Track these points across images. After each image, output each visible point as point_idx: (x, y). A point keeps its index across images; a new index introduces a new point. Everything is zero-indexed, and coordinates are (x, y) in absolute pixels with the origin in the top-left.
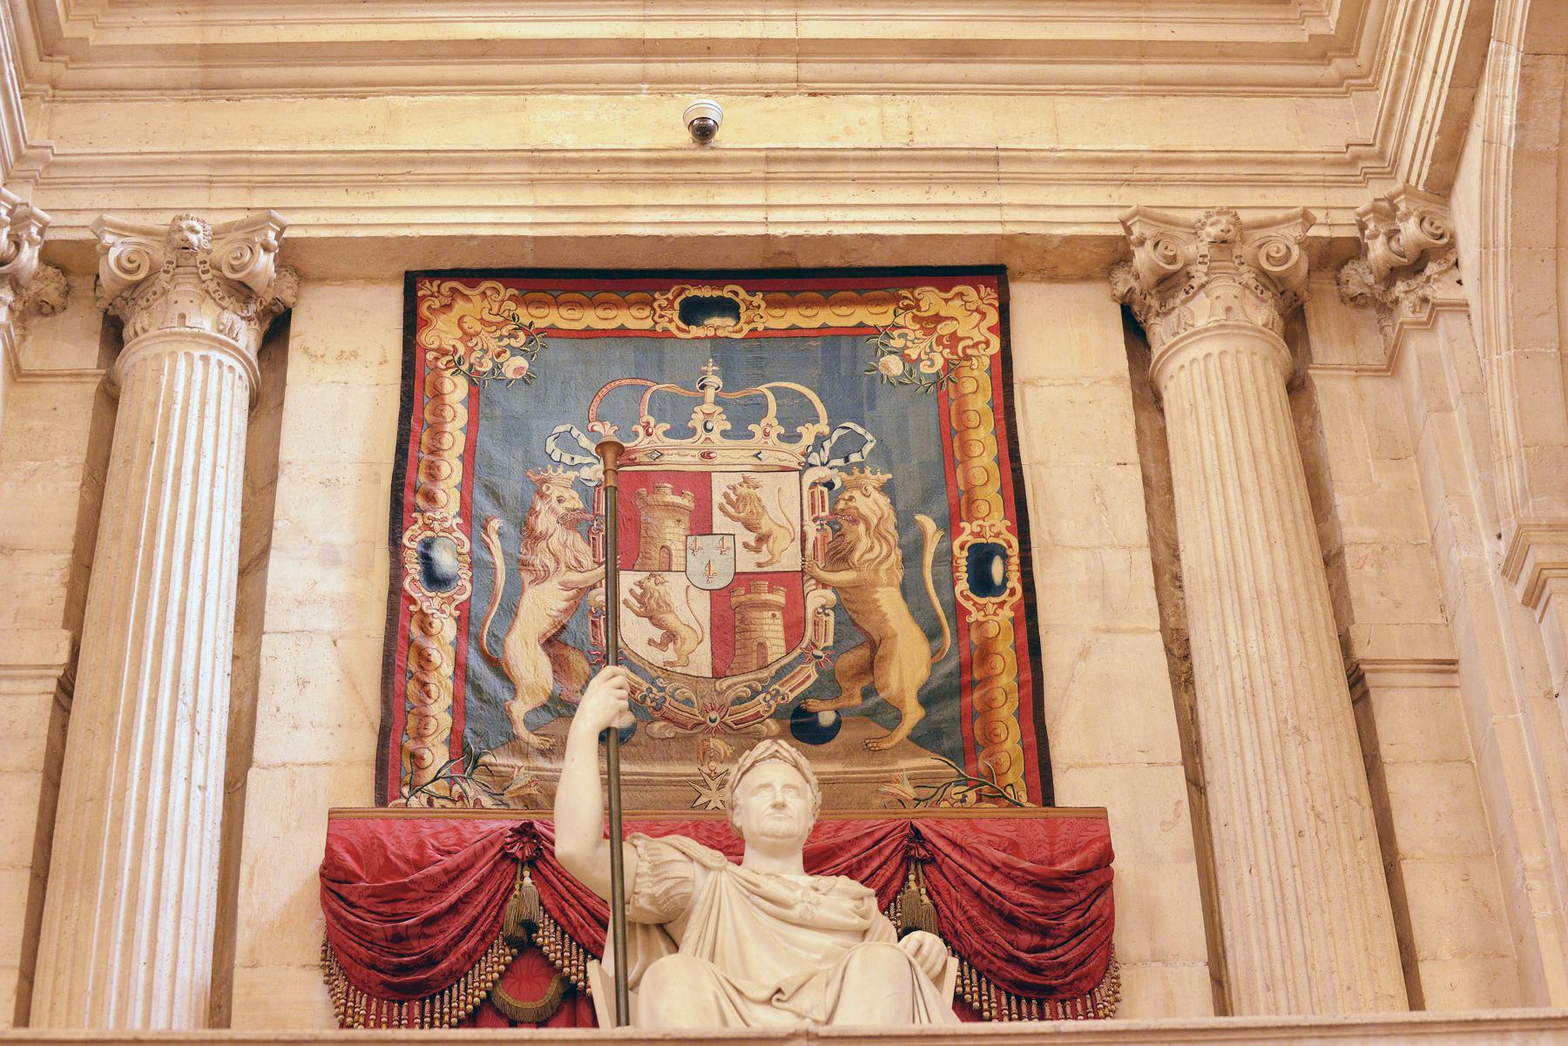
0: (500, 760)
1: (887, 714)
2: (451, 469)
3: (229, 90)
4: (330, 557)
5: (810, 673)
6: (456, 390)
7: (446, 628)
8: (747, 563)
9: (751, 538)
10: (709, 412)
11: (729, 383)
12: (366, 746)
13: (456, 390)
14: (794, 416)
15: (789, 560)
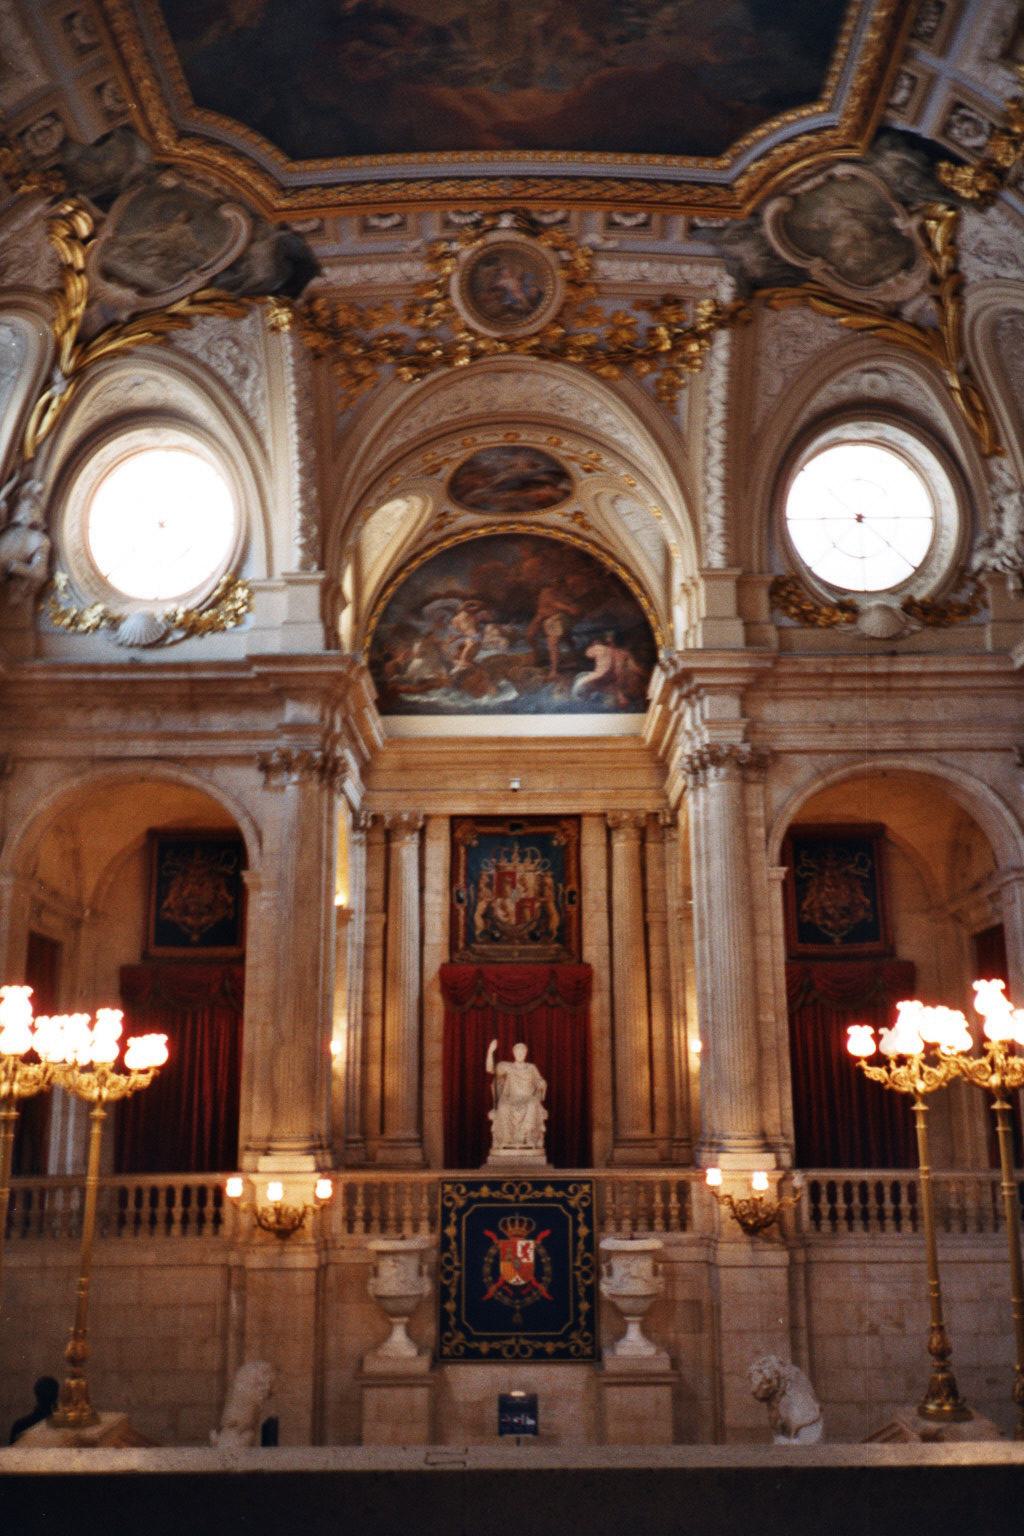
0: (474, 946)
1: (549, 933)
2: (462, 871)
4: (437, 893)
5: (534, 924)
6: (462, 850)
8: (523, 895)
9: (522, 889)
10: (515, 857)
11: (521, 847)
13: (462, 850)
14: (534, 857)
15: (531, 894)
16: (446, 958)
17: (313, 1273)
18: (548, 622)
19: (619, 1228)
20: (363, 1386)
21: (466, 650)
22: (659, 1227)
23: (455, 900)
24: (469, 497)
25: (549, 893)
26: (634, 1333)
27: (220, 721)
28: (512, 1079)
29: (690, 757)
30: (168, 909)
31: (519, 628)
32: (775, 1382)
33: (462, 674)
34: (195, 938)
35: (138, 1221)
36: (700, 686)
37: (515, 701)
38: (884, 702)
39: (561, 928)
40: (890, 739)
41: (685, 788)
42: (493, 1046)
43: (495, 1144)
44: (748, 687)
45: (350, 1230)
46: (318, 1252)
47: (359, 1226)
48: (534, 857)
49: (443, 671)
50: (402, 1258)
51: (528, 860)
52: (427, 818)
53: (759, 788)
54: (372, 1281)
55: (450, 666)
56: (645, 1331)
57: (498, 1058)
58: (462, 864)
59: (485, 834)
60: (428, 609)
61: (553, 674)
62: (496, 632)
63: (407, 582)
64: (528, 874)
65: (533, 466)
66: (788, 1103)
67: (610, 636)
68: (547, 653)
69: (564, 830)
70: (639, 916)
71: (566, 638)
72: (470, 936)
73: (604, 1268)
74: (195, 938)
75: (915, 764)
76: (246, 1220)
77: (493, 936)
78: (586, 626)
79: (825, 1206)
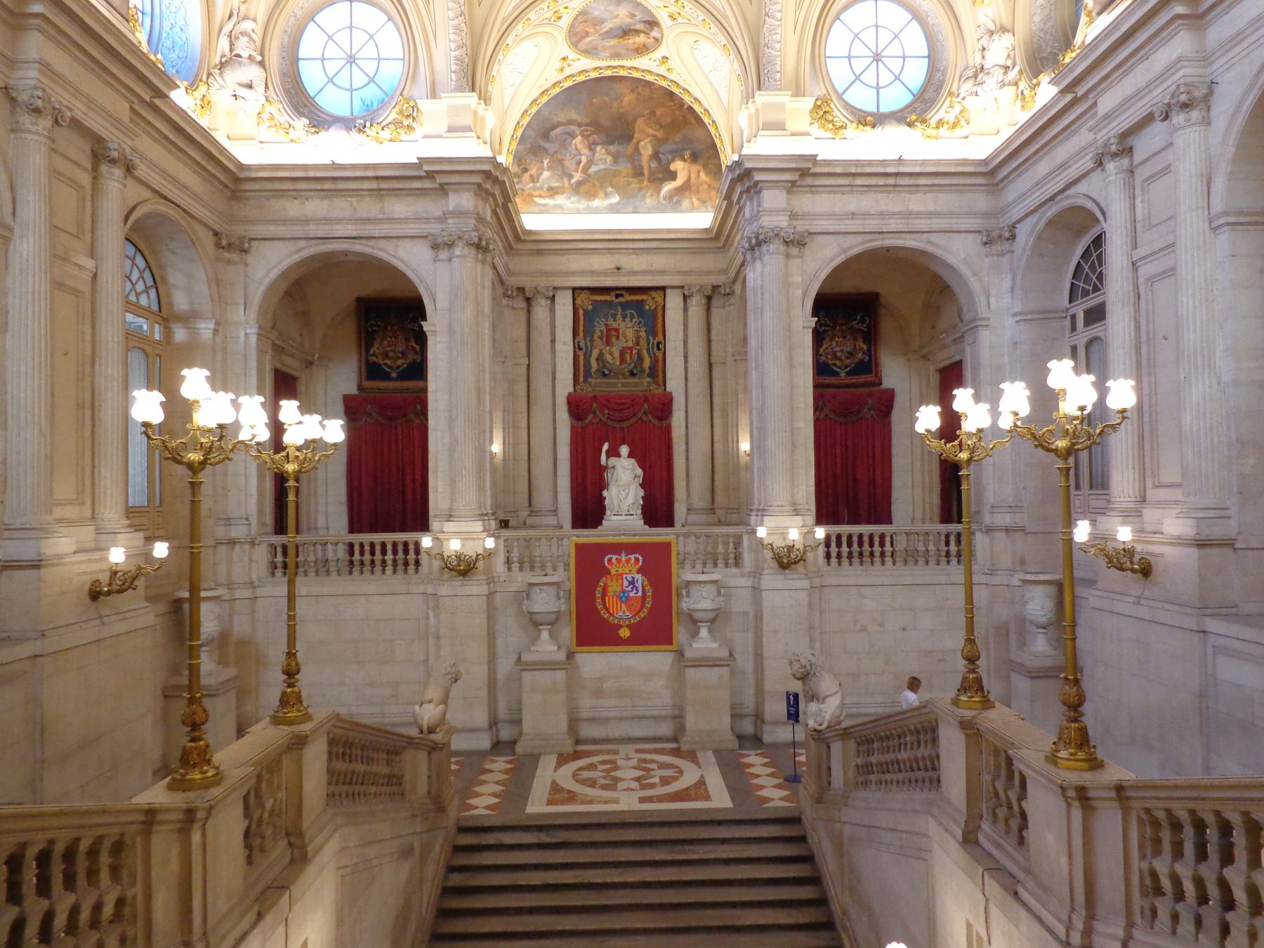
0: (590, 380)
1: (643, 372)
2: (581, 328)
3: (543, 254)
4: (564, 343)
6: (581, 312)
7: (582, 357)
8: (625, 345)
11: (623, 310)
12: (571, 376)
13: (581, 312)
14: (632, 317)
15: (630, 344)
16: (571, 389)
17: (485, 598)
18: (642, 143)
19: (694, 567)
20: (522, 670)
21: (582, 165)
22: (720, 565)
23: (577, 348)
24: (582, 45)
25: (643, 343)
26: (704, 632)
27: (400, 208)
28: (619, 470)
29: (750, 239)
30: (374, 355)
31: (620, 148)
32: (808, 667)
33: (579, 184)
34: (394, 375)
35: (362, 563)
36: (757, 183)
37: (618, 203)
38: (891, 195)
39: (653, 368)
40: (894, 224)
41: (743, 264)
42: (606, 447)
43: (608, 512)
44: (793, 183)
45: (509, 569)
46: (488, 584)
47: (515, 566)
48: (632, 317)
49: (566, 181)
50: (545, 587)
51: (628, 319)
52: (555, 289)
53: (799, 261)
54: (525, 602)
55: (570, 177)
56: (711, 631)
57: (609, 455)
58: (581, 323)
59: (595, 301)
60: (553, 133)
61: (646, 182)
62: (604, 151)
63: (538, 111)
64: (628, 330)
65: (633, 16)
66: (812, 482)
67: (687, 154)
68: (641, 167)
69: (653, 298)
70: (706, 357)
71: (655, 156)
72: (588, 374)
73: (684, 592)
74: (394, 375)
75: (910, 242)
76: (437, 564)
77: (604, 373)
78: (669, 146)
79: (834, 549)
